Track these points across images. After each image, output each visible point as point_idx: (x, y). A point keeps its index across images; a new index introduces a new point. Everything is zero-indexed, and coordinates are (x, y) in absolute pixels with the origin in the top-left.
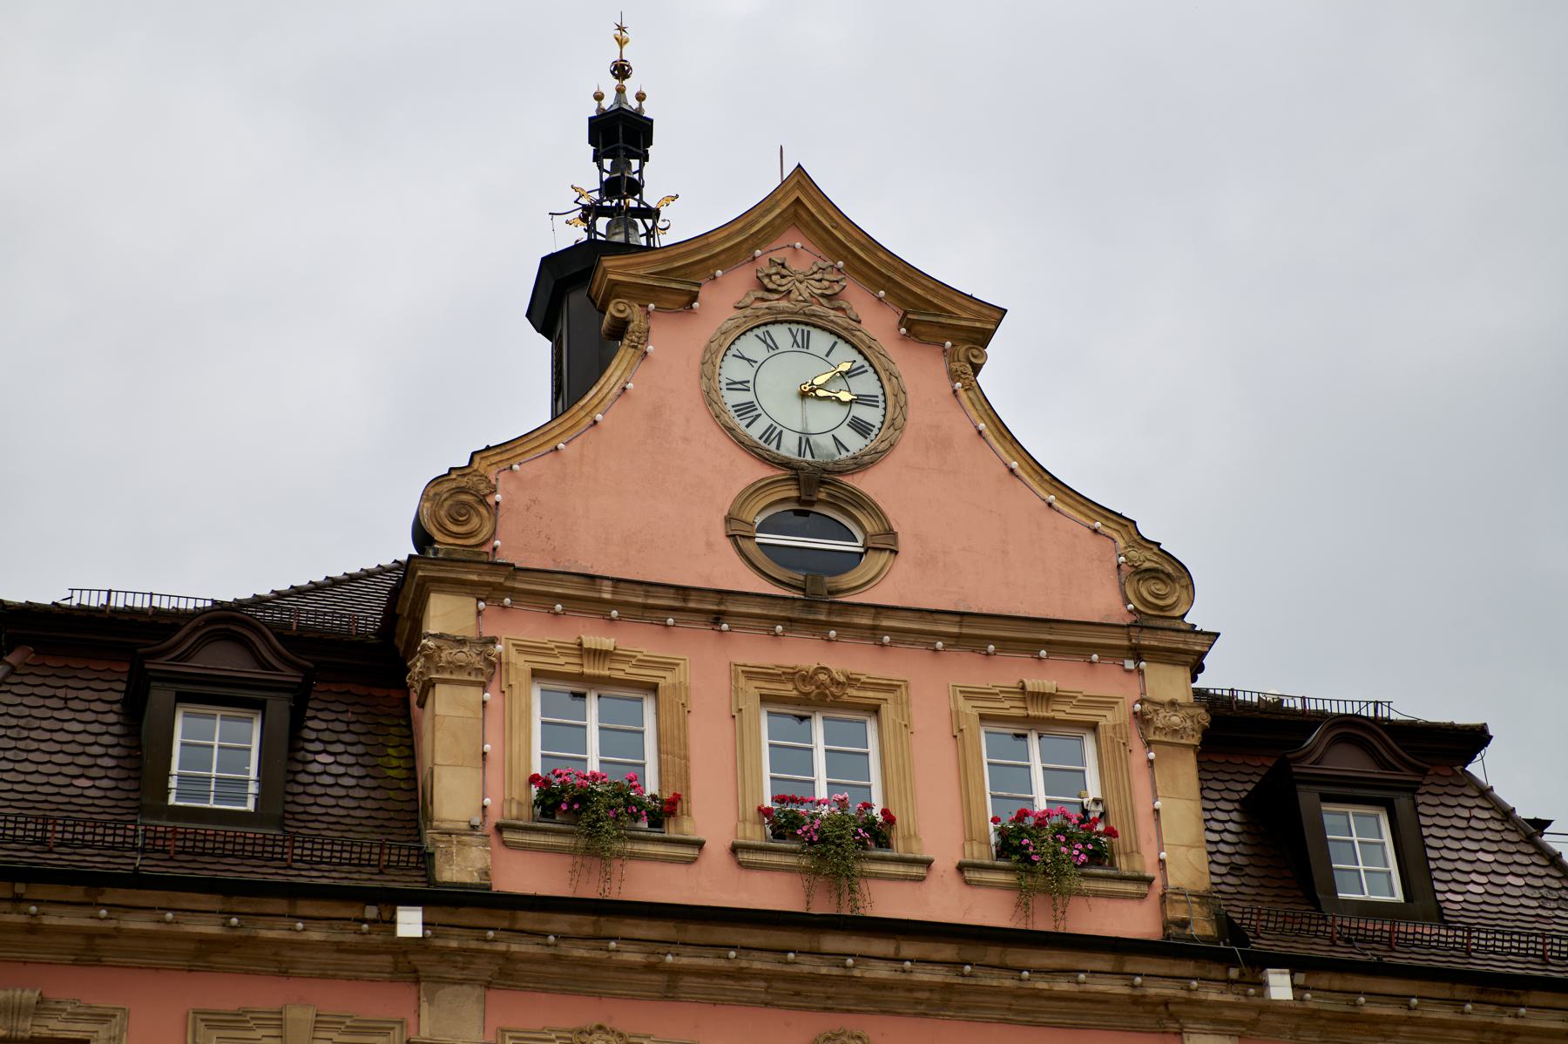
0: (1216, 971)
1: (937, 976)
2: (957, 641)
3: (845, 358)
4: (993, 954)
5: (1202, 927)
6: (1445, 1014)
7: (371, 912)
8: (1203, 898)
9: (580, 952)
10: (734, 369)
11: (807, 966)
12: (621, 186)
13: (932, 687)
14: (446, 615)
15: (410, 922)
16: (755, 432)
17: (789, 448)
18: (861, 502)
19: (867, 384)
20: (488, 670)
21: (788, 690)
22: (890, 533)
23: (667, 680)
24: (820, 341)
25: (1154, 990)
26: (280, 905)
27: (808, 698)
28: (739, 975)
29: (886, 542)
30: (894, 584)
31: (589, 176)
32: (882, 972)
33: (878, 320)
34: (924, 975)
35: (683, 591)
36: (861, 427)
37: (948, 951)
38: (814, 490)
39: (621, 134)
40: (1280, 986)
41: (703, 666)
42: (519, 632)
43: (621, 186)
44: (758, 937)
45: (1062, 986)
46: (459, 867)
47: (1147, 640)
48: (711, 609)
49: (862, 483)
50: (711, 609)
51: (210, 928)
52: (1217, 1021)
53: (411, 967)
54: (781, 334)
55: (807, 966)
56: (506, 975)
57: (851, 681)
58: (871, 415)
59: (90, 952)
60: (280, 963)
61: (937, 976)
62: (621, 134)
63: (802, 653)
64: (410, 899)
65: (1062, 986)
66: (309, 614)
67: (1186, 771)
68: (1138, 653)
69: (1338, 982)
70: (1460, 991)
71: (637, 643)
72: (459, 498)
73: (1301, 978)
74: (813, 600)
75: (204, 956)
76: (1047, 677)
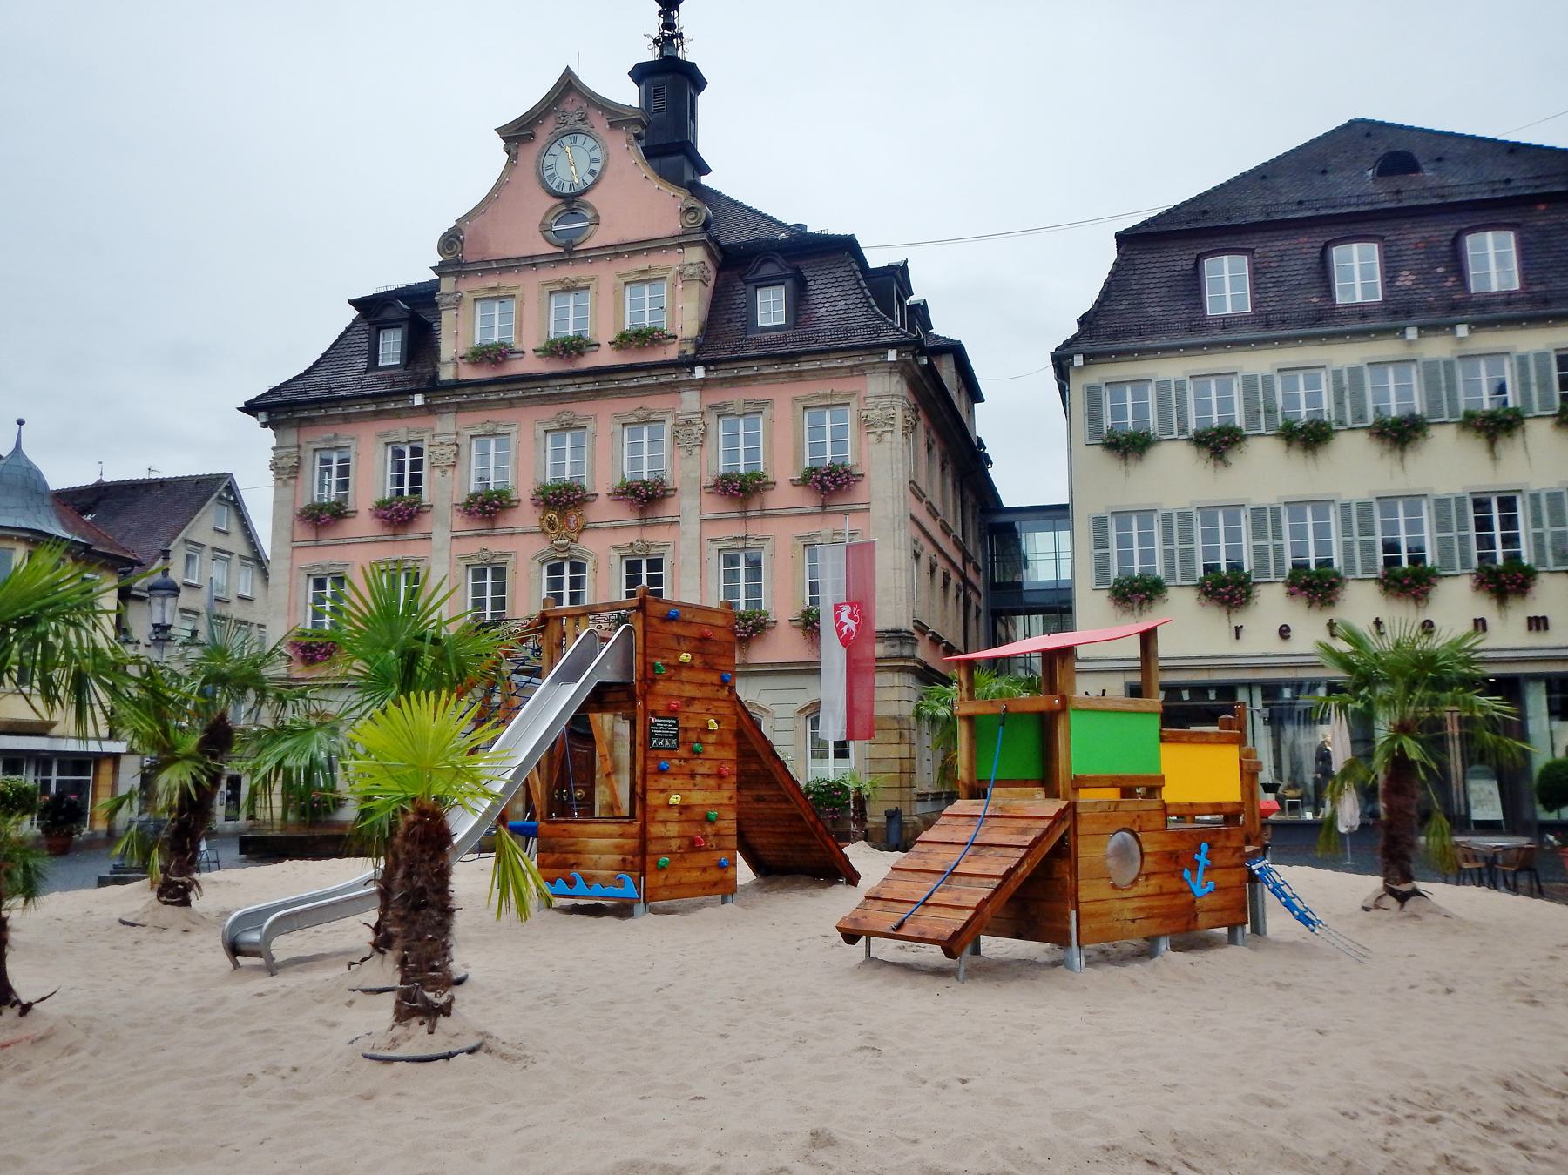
2: (617, 255)
3: (590, 143)
4: (606, 377)
5: (691, 352)
10: (549, 160)
13: (606, 274)
14: (447, 285)
16: (554, 186)
17: (566, 191)
18: (586, 205)
19: (596, 154)
21: (558, 287)
22: (597, 216)
23: (518, 292)
24: (580, 138)
28: (529, 397)
29: (596, 221)
30: (601, 237)
32: (571, 389)
33: (599, 123)
35: (518, 259)
36: (592, 173)
37: (591, 379)
38: (570, 203)
40: (700, 372)
41: (528, 284)
44: (530, 385)
46: (446, 374)
48: (531, 262)
50: (531, 262)
54: (566, 140)
55: (548, 391)
56: (460, 408)
57: (578, 280)
58: (597, 167)
60: (395, 414)
65: (632, 384)
68: (680, 245)
71: (508, 281)
72: (450, 241)
74: (569, 252)
76: (641, 263)
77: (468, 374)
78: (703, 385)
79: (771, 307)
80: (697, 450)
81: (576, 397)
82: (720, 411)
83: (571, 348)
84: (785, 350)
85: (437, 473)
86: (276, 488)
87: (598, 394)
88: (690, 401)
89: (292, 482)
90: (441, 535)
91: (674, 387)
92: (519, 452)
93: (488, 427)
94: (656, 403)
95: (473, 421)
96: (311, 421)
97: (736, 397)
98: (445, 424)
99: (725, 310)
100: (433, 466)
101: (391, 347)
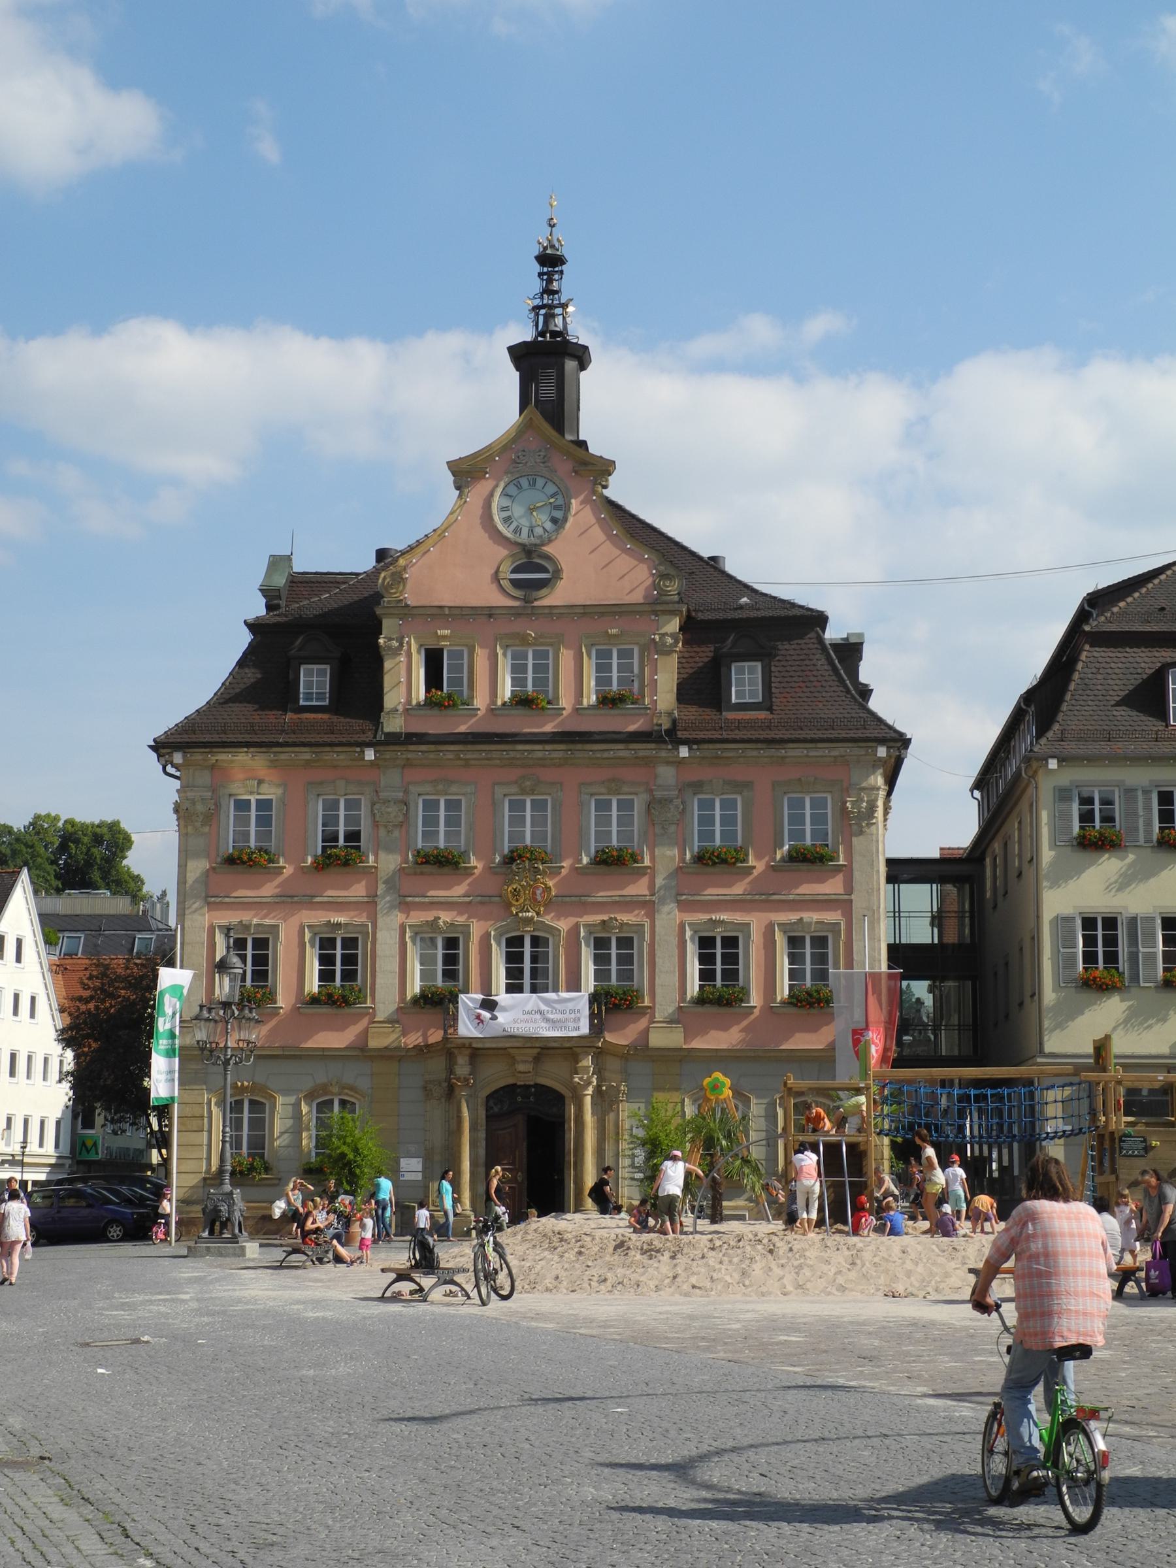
0: (664, 746)
1: (560, 755)
6: (755, 753)
7: (358, 749)
8: (670, 714)
9: (432, 756)
11: (512, 754)
15: (370, 754)
18: (548, 557)
25: (641, 754)
26: (328, 749)
32: (540, 755)
34: (555, 755)
45: (606, 755)
46: (393, 724)
47: (659, 608)
48: (490, 613)
49: (548, 549)
51: (307, 757)
52: (668, 763)
55: (512, 754)
61: (560, 755)
64: (369, 745)
65: (606, 755)
68: (655, 613)
69: (711, 746)
70: (759, 746)
73: (695, 747)
75: (308, 764)
79: (745, 682)
80: (673, 828)
84: (771, 735)
85: (382, 832)
86: (184, 836)
88: (667, 774)
89: (206, 829)
91: (649, 763)
93: (440, 787)
99: (703, 688)
100: (376, 824)
101: (314, 682)
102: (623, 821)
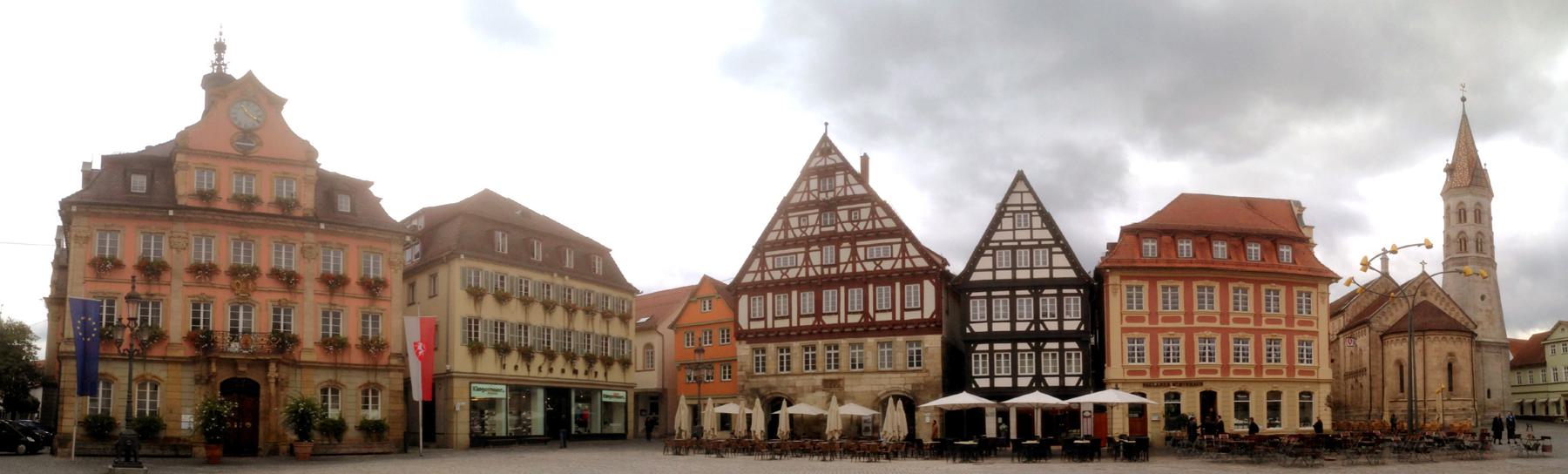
12: (220, 59)
14: (180, 158)
20: (187, 167)
27: (243, 172)
31: (214, 57)
39: (220, 48)
40: (322, 226)
41: (224, 166)
42: (193, 161)
43: (220, 59)
46: (181, 202)
48: (226, 156)
53: (171, 219)
56: (189, 220)
59: (120, 217)
60: (150, 218)
62: (220, 48)
63: (242, 165)
66: (159, 154)
67: (312, 187)
75: (137, 217)
77: (191, 203)
78: (318, 232)
81: (251, 226)
82: (324, 244)
83: (250, 201)
87: (264, 226)
88: (310, 237)
90: (177, 284)
91: (301, 230)
92: (221, 249)
94: (294, 235)
95: (196, 228)
96: (98, 215)
97: (334, 240)
98: (180, 228)
102: (289, 255)
